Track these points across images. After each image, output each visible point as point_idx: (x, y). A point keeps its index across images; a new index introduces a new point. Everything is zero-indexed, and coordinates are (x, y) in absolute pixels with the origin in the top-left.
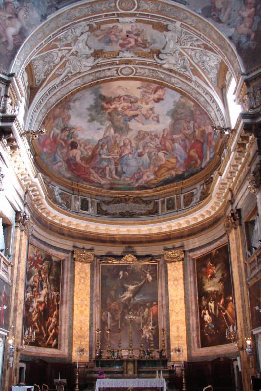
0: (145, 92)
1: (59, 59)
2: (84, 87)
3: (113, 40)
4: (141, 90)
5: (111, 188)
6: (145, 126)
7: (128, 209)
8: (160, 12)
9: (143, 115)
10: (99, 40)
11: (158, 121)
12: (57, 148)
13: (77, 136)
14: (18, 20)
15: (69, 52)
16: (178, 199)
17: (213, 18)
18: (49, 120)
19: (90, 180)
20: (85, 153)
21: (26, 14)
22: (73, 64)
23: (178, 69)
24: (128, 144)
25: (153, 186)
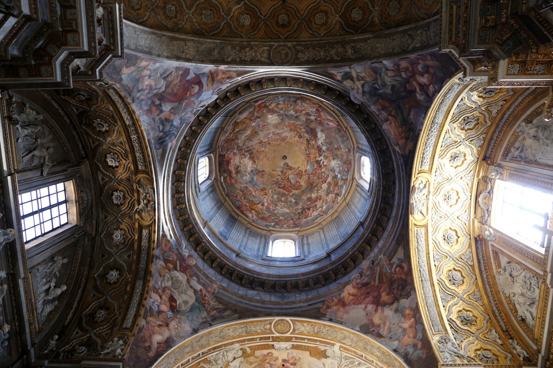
8: (316, 335)
14: (168, 329)
17: (372, 334)
21: (177, 325)
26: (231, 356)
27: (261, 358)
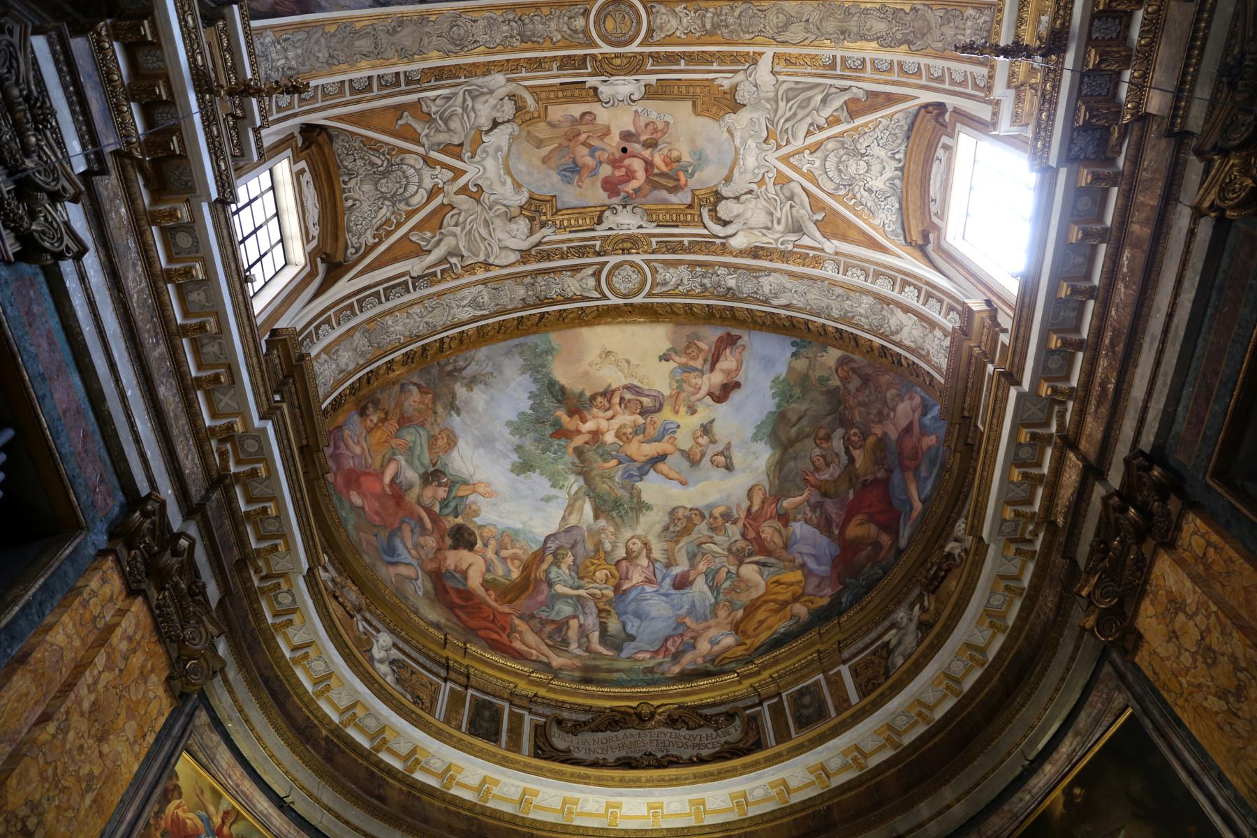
0: (686, 369)
1: (422, 196)
2: (501, 325)
3: (585, 166)
4: (671, 365)
5: (587, 681)
6: (691, 489)
7: (650, 749)
8: (709, 35)
9: (682, 452)
10: (545, 160)
11: (729, 467)
12: (402, 522)
13: (477, 513)
15: (454, 180)
16: (836, 683)
18: (383, 416)
19: (513, 649)
20: (500, 570)
22: (468, 227)
23: (776, 240)
24: (640, 553)
25: (733, 665)
26: (484, 111)
27: (566, 127)
